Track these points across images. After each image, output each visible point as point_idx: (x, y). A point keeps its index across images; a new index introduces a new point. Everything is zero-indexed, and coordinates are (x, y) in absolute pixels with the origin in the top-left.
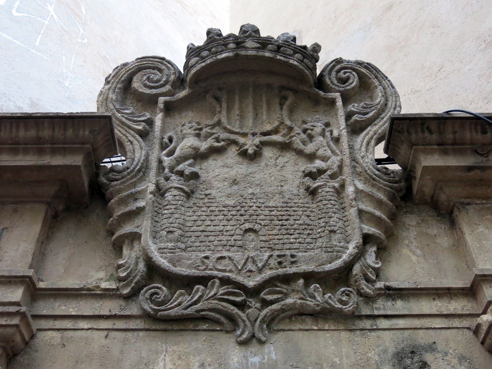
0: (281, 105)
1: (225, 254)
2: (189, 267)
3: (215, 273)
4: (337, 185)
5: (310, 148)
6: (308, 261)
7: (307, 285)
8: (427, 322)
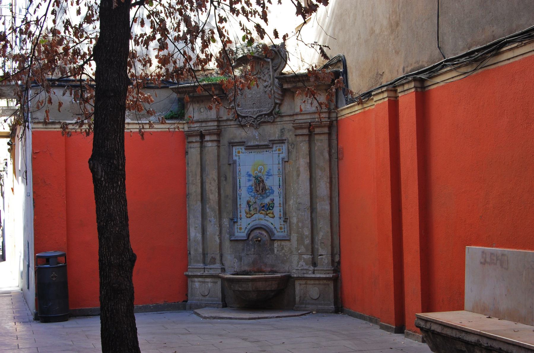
0: (258, 64)
1: (250, 110)
2: (244, 114)
3: (248, 115)
4: (270, 90)
5: (264, 79)
6: (265, 111)
7: (265, 116)
8: (287, 122)
